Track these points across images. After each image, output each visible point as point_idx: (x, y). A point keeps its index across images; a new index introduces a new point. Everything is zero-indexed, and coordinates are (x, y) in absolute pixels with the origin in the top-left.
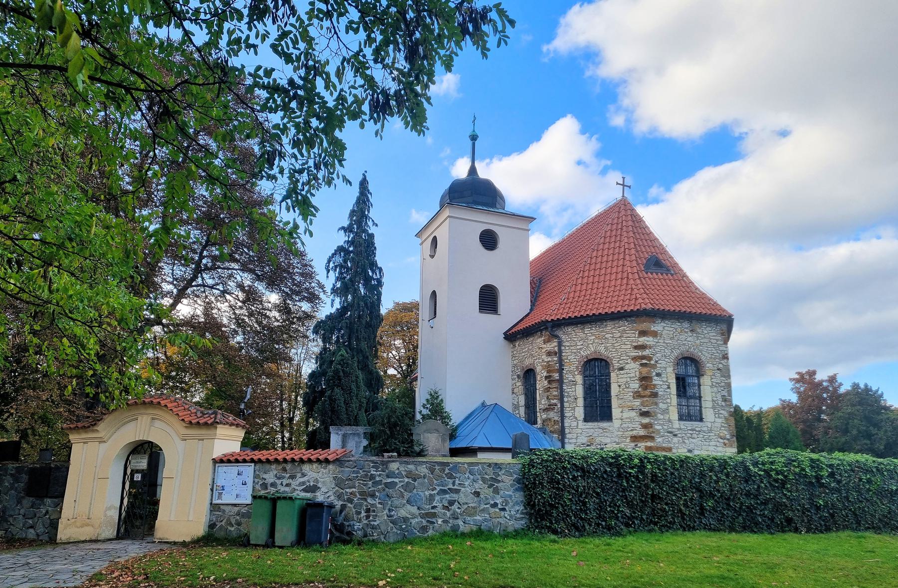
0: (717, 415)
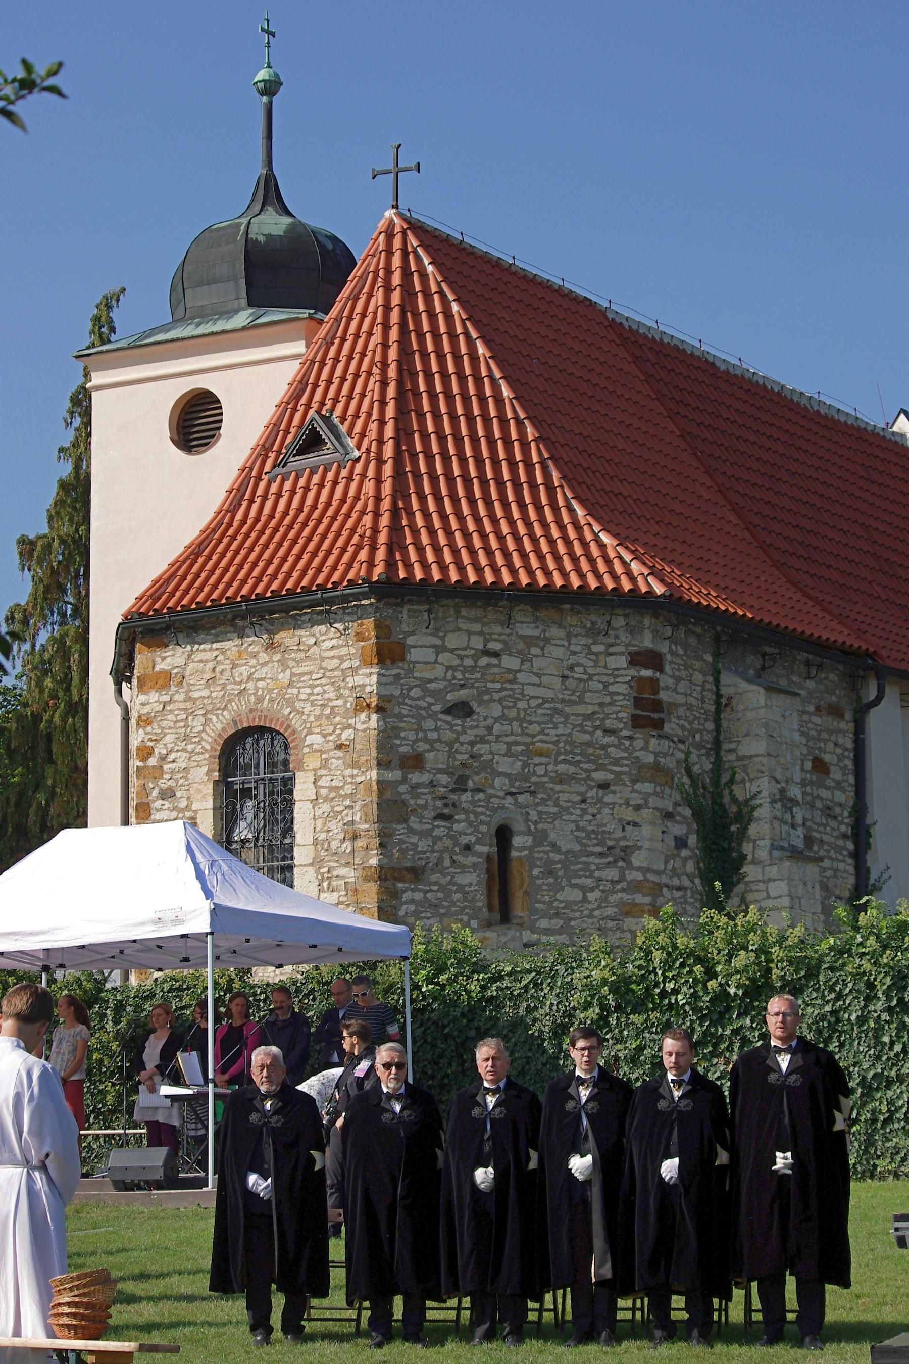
0: (325, 882)
